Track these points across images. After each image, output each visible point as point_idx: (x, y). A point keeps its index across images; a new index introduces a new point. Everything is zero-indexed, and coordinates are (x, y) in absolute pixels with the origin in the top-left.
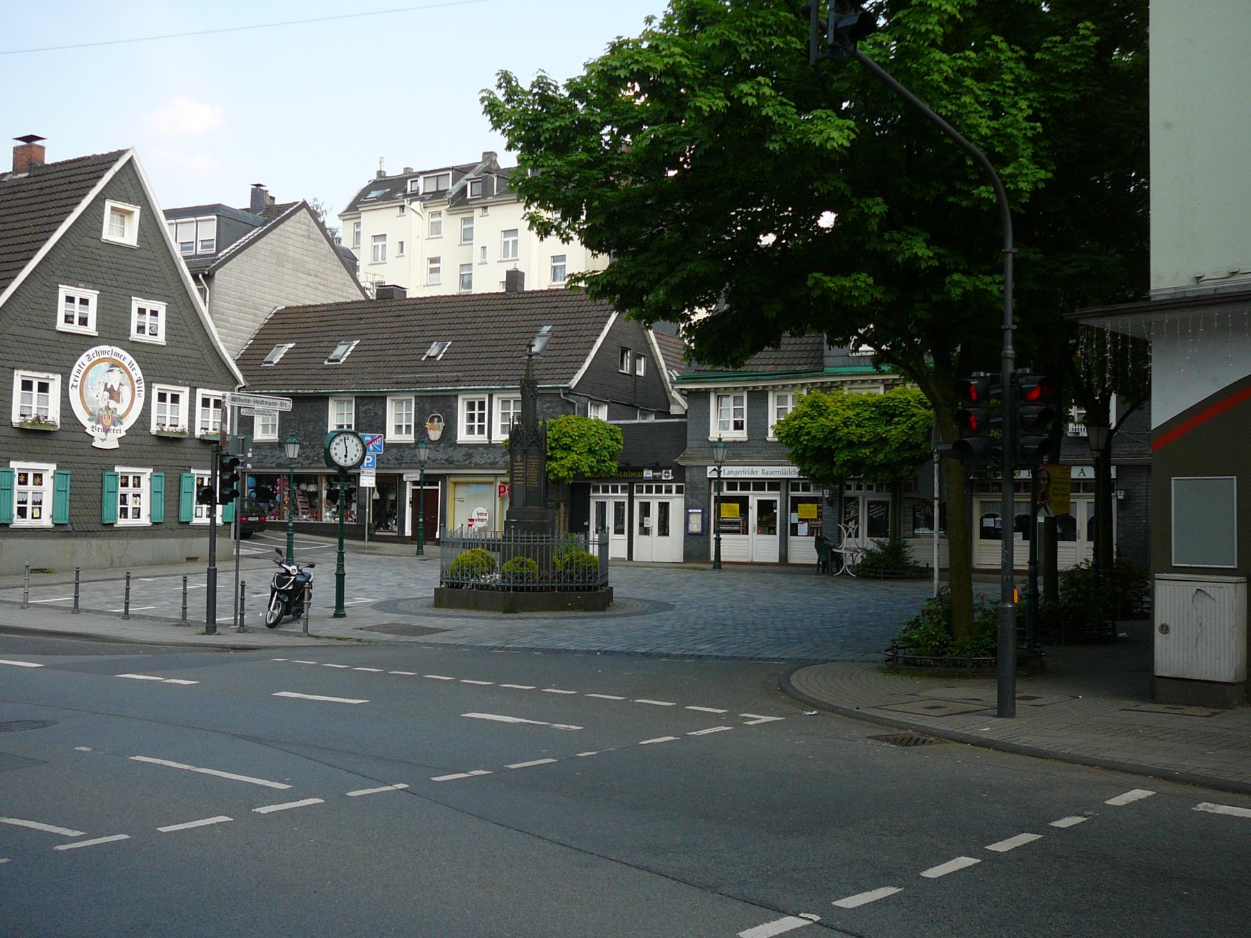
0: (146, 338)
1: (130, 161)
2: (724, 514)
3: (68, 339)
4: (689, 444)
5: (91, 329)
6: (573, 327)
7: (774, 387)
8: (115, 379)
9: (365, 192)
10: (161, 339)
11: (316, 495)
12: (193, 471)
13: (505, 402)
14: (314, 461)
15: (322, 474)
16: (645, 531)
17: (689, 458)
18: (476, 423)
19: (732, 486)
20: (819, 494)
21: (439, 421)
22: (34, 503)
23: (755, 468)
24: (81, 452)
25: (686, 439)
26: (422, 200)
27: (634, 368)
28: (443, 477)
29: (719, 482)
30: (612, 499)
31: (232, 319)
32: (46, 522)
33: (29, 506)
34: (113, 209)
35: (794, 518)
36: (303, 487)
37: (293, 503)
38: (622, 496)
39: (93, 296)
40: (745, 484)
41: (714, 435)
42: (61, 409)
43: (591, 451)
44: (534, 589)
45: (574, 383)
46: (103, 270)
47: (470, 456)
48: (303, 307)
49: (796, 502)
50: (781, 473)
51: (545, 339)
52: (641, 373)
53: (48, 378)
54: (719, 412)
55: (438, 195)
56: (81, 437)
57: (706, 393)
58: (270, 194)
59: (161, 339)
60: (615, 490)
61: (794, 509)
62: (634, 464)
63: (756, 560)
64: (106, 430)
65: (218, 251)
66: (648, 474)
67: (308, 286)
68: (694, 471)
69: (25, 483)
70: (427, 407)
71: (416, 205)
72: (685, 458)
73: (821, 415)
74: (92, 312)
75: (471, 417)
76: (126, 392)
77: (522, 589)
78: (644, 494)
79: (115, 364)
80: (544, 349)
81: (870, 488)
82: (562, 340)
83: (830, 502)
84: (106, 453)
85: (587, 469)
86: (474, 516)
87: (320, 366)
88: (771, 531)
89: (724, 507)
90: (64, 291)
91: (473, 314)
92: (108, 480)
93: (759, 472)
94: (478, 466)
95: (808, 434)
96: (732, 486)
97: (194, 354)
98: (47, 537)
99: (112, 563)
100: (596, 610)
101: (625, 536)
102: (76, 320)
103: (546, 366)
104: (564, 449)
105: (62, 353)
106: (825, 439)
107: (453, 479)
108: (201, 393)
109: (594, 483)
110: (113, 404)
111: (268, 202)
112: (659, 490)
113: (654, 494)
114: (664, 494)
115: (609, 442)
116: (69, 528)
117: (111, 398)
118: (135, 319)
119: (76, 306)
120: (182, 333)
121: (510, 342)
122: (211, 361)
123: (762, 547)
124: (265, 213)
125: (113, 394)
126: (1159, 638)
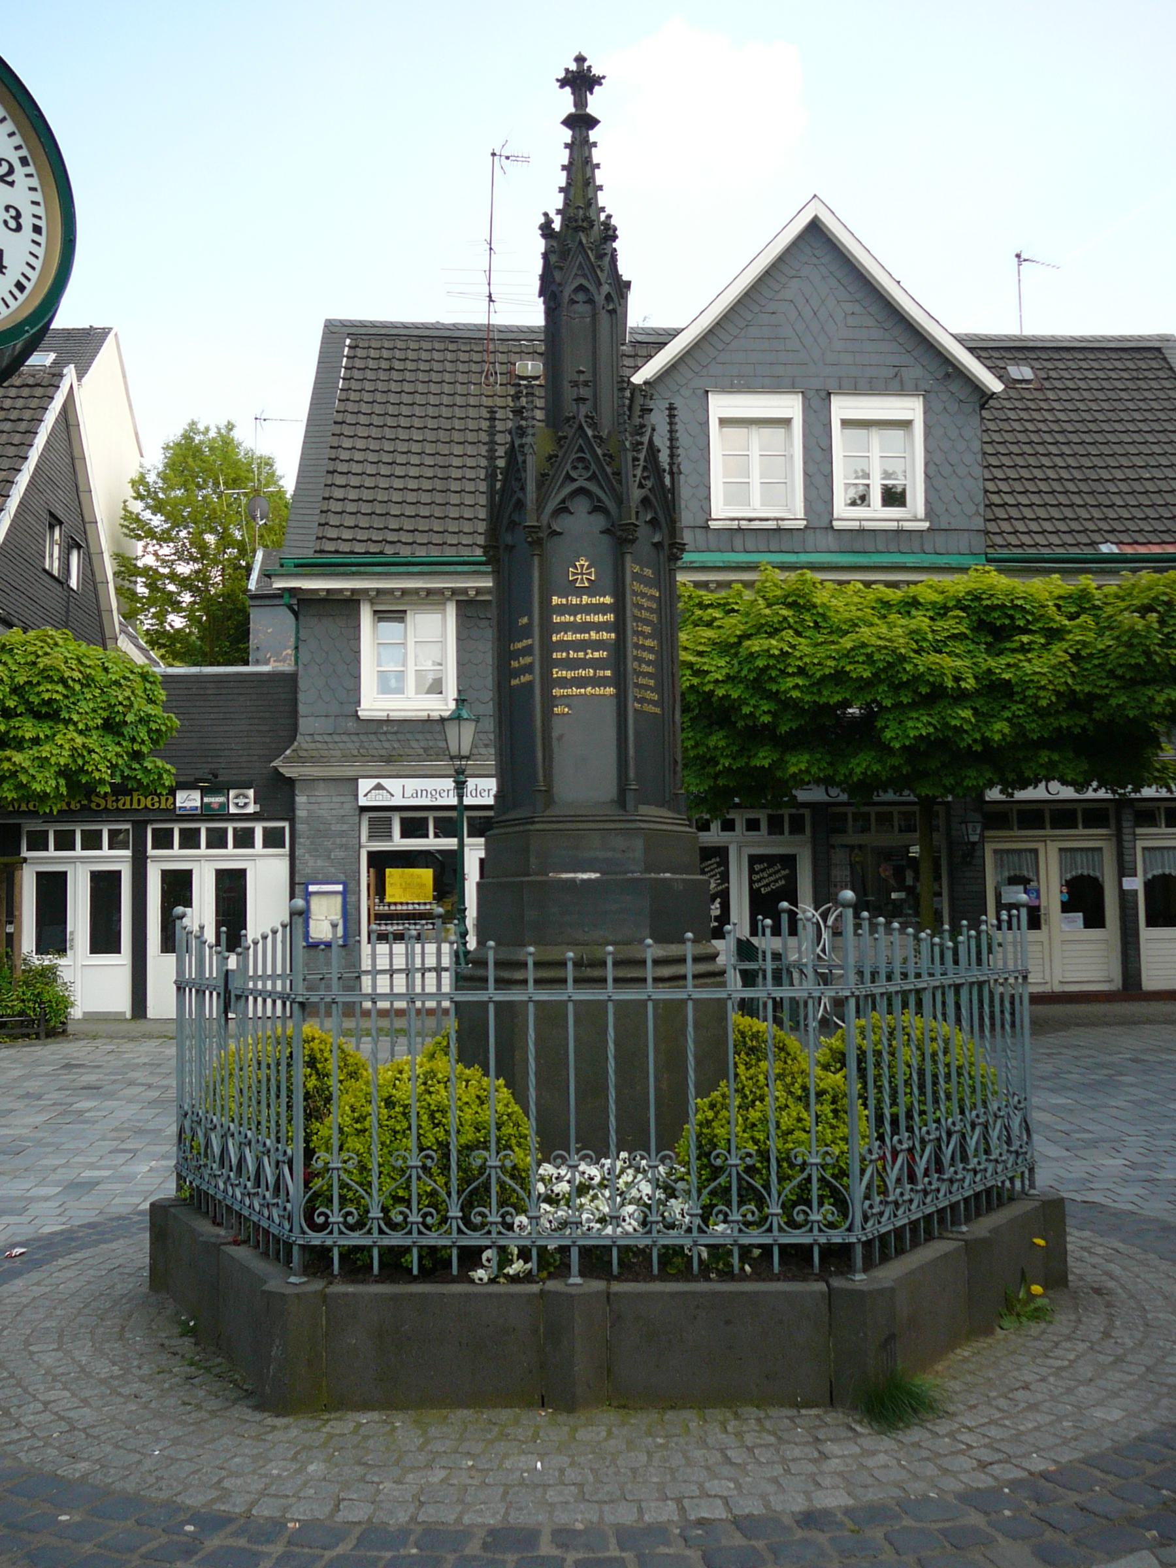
2: (394, 893)
19: (413, 828)
25: (294, 714)
29: (379, 817)
57: (348, 605)
60: (92, 841)
66: (188, 800)
72: (300, 759)
81: (753, 825)
101: (123, 959)
104: (38, 716)
109: (30, 825)
112: (217, 840)
113: (203, 850)
114: (230, 850)
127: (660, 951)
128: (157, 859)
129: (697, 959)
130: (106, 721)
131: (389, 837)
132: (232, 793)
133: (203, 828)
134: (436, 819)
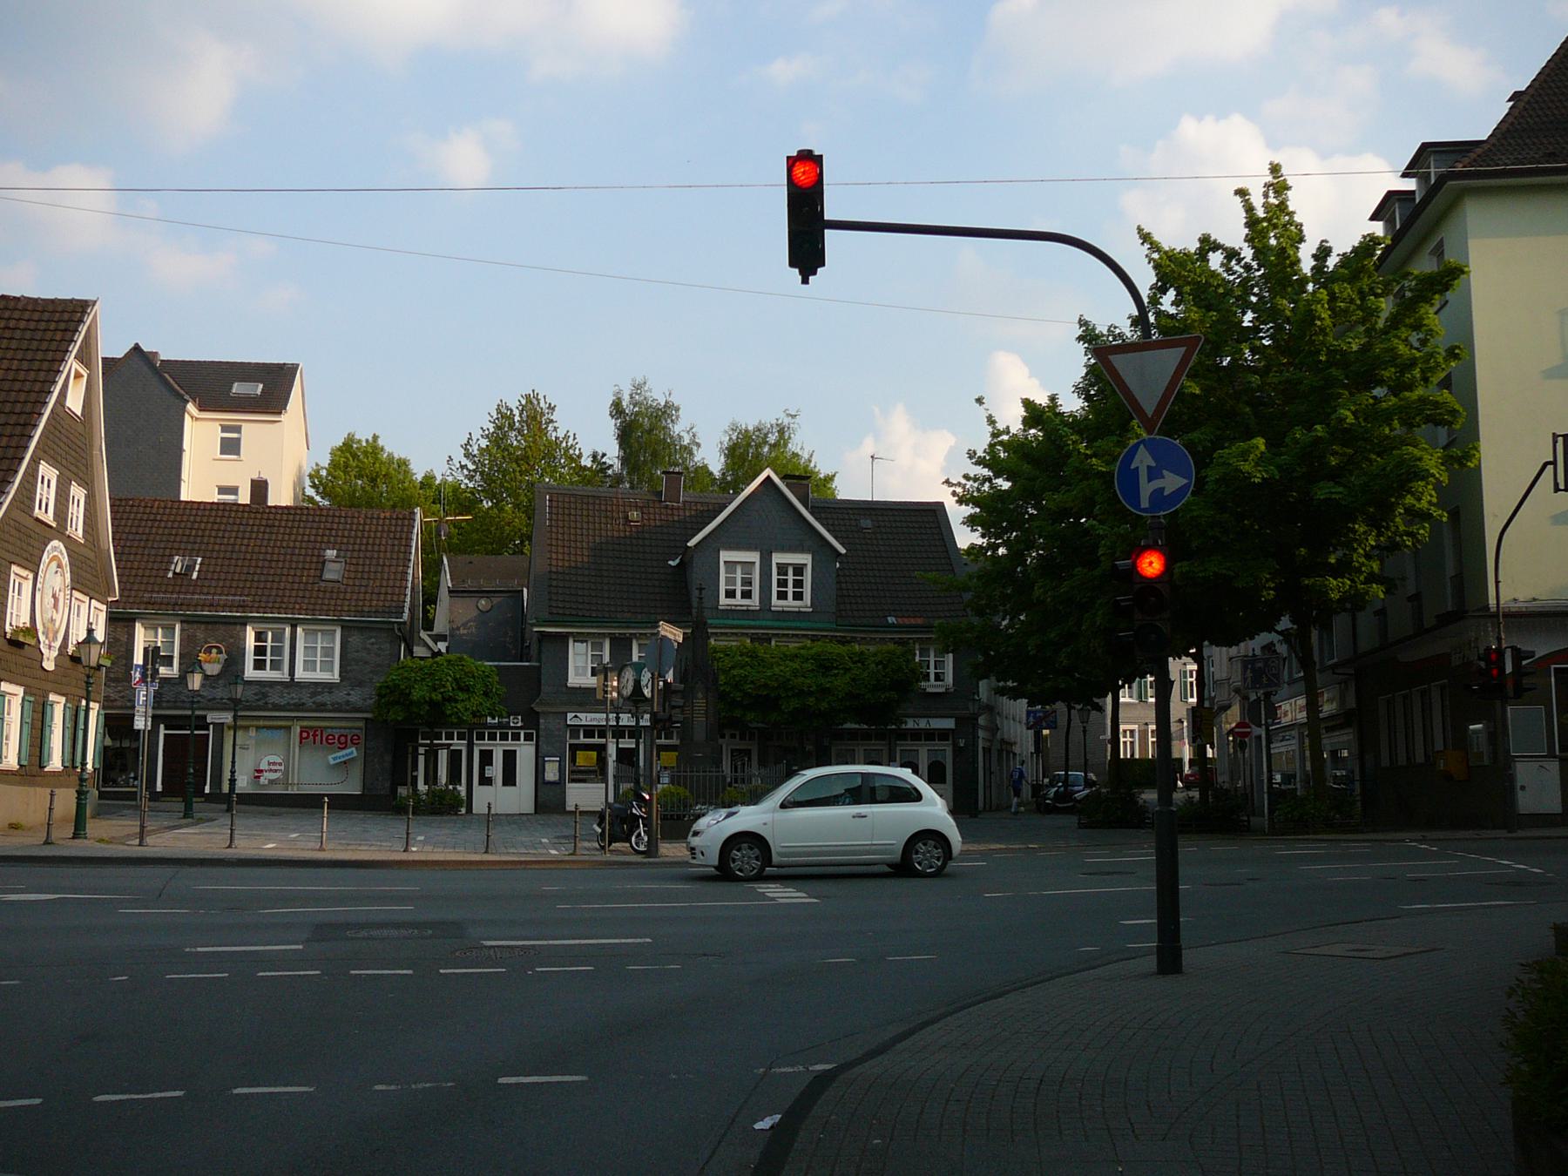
4: (545, 688)
21: (220, 652)
29: (575, 730)
38: (459, 744)
41: (574, 680)
70: (200, 635)
94: (277, 707)
112: (504, 737)
126: (1520, 794)
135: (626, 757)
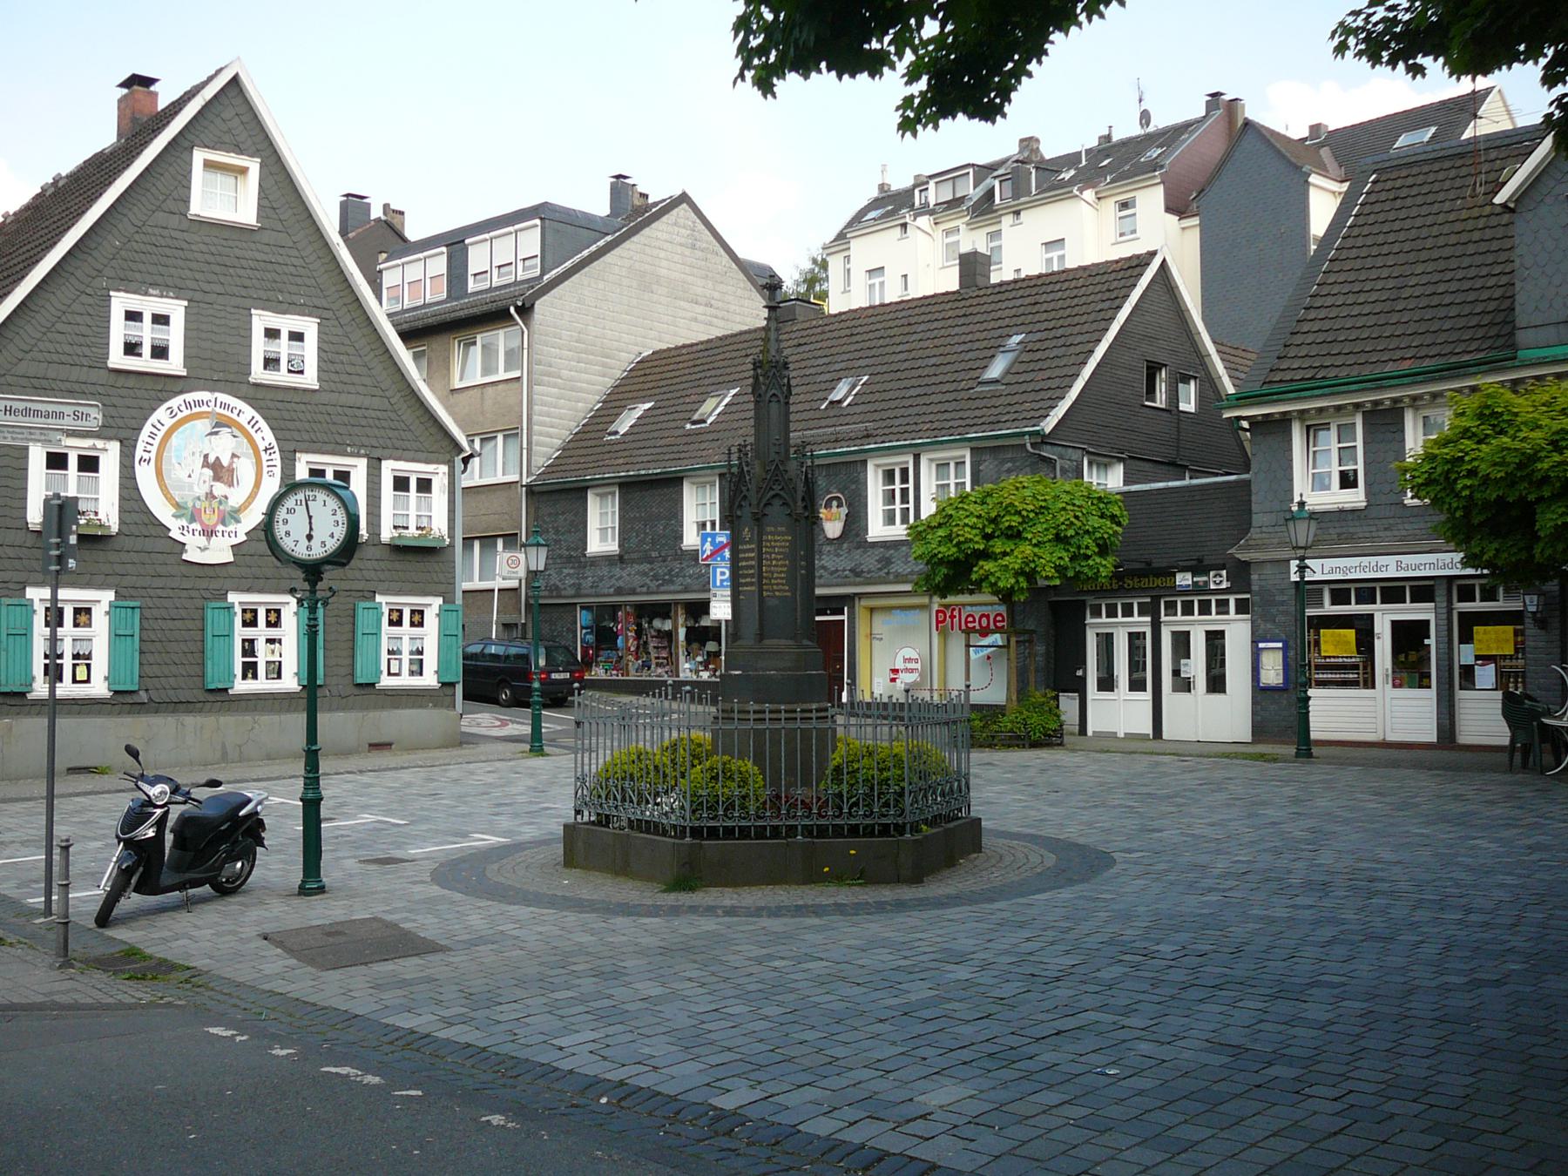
0: (281, 377)
1: (235, 80)
3: (131, 382)
4: (1257, 519)
5: (175, 364)
6: (1060, 332)
7: (1415, 398)
8: (223, 446)
9: (858, 219)
10: (310, 379)
11: (669, 636)
12: (379, 598)
13: (942, 466)
14: (665, 582)
15: (677, 603)
16: (1184, 685)
17: (1257, 547)
18: (898, 506)
19: (1340, 596)
20: (1514, 606)
22: (76, 656)
23: (1383, 560)
24: (162, 570)
25: (1250, 511)
26: (932, 212)
27: (1174, 397)
28: (849, 599)
30: (1123, 627)
31: (565, 373)
32: (98, 688)
33: (67, 662)
34: (208, 165)
35: (1466, 655)
36: (657, 623)
37: (643, 647)
38: (1141, 623)
39: (176, 309)
40: (1366, 590)
42: (122, 498)
43: (1059, 539)
44: (744, 833)
45: (1049, 425)
46: (194, 265)
47: (887, 562)
48: (677, 348)
49: (1469, 622)
50: (1417, 567)
51: (1011, 356)
52: (1188, 405)
53: (94, 448)
54: (1313, 458)
55: (955, 203)
56: (160, 545)
57: (1284, 422)
58: (640, 189)
59: (310, 379)
60: (1128, 612)
61: (1466, 638)
62: (1158, 563)
63: (1391, 737)
64: (209, 533)
65: (543, 273)
66: (1184, 579)
67: (695, 320)
68: (1268, 570)
69: (399, 623)
71: (924, 221)
72: (1248, 547)
73: (1502, 432)
74: (175, 336)
75: (890, 497)
76: (245, 470)
77: (713, 833)
78: (1179, 617)
79: (221, 423)
80: (1007, 372)
82: (1038, 355)
83: (1541, 622)
84: (210, 572)
85: (1050, 572)
86: (899, 665)
87: (680, 432)
88: (1422, 682)
89: (1314, 639)
90: (120, 302)
91: (907, 329)
92: (213, 618)
93: (1389, 567)
95: (1472, 473)
96: (1340, 596)
97: (376, 402)
98: (99, 713)
99: (225, 754)
100: (897, 880)
101: (1147, 696)
102: (146, 350)
103: (1009, 399)
104: (1009, 537)
105: (129, 403)
106: (1511, 481)
107: (865, 603)
108: (389, 468)
109: (1091, 600)
110: (220, 489)
111: (637, 202)
112: (1205, 609)
113: (1196, 617)
115: (1095, 521)
116: (143, 696)
117: (217, 478)
118: (259, 347)
119: (145, 324)
120: (349, 369)
121: (957, 367)
122: (409, 415)
123: (1395, 712)
124: (632, 212)
125: (221, 472)
127: (757, 707)
128: (1169, 623)
129: (818, 710)
130: (1057, 535)
131: (1321, 605)
132: (1212, 573)
133: (1196, 599)
134: (1382, 589)
135: (1408, 637)
